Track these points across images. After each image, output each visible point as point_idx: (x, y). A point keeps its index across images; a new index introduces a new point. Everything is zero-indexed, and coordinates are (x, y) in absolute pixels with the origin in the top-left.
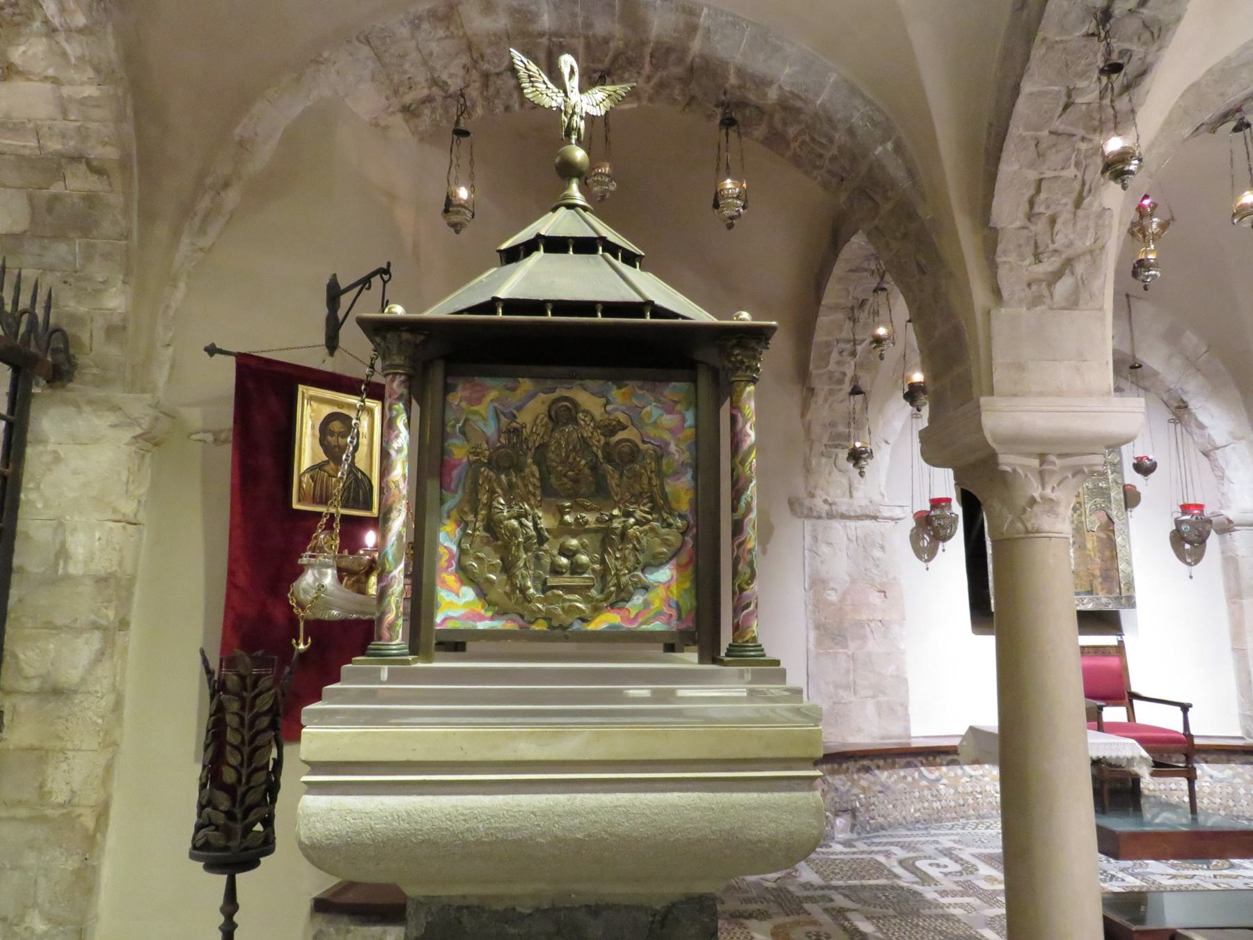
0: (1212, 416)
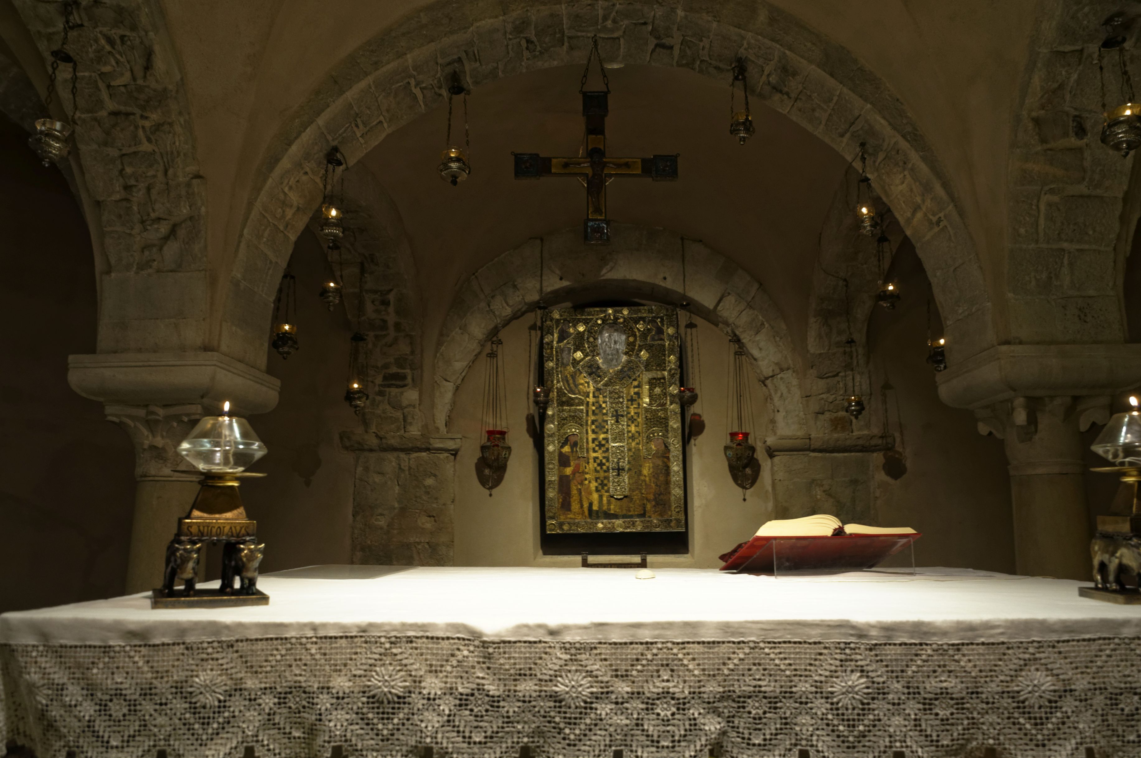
0: (760, 349)
